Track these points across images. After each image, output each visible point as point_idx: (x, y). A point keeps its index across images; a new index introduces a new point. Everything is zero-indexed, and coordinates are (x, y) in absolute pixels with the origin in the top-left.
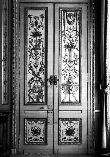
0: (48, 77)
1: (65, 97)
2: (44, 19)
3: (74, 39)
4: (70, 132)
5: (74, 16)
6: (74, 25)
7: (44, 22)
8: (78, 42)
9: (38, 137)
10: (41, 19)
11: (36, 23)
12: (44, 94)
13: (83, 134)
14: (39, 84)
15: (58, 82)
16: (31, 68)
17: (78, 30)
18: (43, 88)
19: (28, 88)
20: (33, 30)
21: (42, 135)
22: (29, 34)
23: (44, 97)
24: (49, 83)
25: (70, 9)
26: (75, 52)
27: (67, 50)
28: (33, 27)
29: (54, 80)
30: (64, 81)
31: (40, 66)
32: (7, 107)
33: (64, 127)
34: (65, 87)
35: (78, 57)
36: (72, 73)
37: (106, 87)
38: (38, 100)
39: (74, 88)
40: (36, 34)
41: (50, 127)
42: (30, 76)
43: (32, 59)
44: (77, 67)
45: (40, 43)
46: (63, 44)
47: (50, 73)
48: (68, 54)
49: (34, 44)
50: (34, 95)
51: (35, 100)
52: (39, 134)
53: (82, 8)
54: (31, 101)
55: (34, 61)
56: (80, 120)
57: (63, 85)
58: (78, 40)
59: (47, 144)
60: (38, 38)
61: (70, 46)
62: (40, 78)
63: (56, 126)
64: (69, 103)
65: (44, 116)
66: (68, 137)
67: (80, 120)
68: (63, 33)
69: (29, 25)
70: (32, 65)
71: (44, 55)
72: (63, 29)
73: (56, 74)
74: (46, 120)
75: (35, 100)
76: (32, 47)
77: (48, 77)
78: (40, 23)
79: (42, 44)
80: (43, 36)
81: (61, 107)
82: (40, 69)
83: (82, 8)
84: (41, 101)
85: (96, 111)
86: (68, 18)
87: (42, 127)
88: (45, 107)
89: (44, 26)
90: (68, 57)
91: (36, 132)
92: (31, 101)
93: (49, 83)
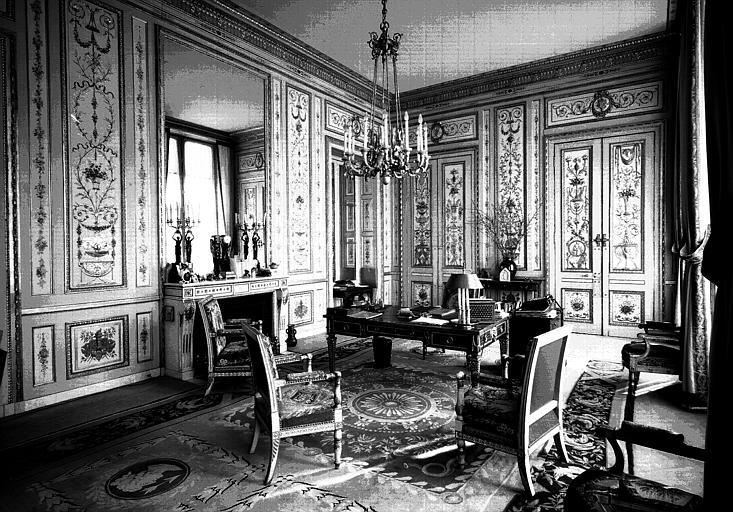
0: (594, 237)
1: (618, 262)
2: (587, 161)
3: (633, 184)
4: (626, 310)
5: (632, 151)
6: (633, 164)
7: (587, 165)
8: (639, 187)
9: (580, 313)
10: (583, 161)
11: (576, 167)
12: (587, 257)
13: (646, 310)
14: (581, 245)
15: (607, 243)
16: (569, 225)
17: (639, 170)
18: (587, 251)
19: (567, 251)
20: (572, 177)
21: (586, 310)
22: (448, 191)
23: (588, 262)
24: (594, 244)
25: (626, 143)
26: (635, 201)
27: (622, 199)
28: (572, 172)
29: (602, 241)
30: (616, 239)
31: (581, 223)
32: (538, 274)
33: (618, 301)
34: (620, 250)
35: (639, 208)
36: (629, 230)
37: (694, 248)
38: (580, 265)
39: (633, 249)
40: (576, 182)
41: (597, 300)
42: (568, 236)
43: (571, 214)
44: (638, 222)
45: (581, 193)
46: (615, 192)
47: (596, 231)
48: (623, 205)
49: (574, 195)
50: (575, 260)
51: (576, 266)
52: (581, 308)
53: (644, 140)
54: (570, 266)
55: (574, 216)
56: (642, 294)
57: (616, 247)
58: (640, 184)
59: (592, 322)
60: (579, 186)
61: (627, 194)
62: (582, 239)
63: (606, 299)
64: (625, 270)
65: (589, 287)
66: (623, 316)
67: (642, 294)
68: (616, 177)
69: (566, 172)
70: (572, 222)
71: (588, 207)
72: (616, 172)
73: (606, 232)
74: (591, 292)
75: (576, 266)
76: (571, 198)
77: (594, 237)
78: (581, 167)
79: (586, 194)
80: (587, 184)
81: (612, 276)
82: (583, 226)
83: (644, 140)
84: (583, 266)
85: (667, 282)
86: (624, 156)
87: (428, 291)
88: (590, 275)
89: (588, 171)
90: (623, 209)
91: (577, 306)
92: (570, 266)
93: (594, 244)
